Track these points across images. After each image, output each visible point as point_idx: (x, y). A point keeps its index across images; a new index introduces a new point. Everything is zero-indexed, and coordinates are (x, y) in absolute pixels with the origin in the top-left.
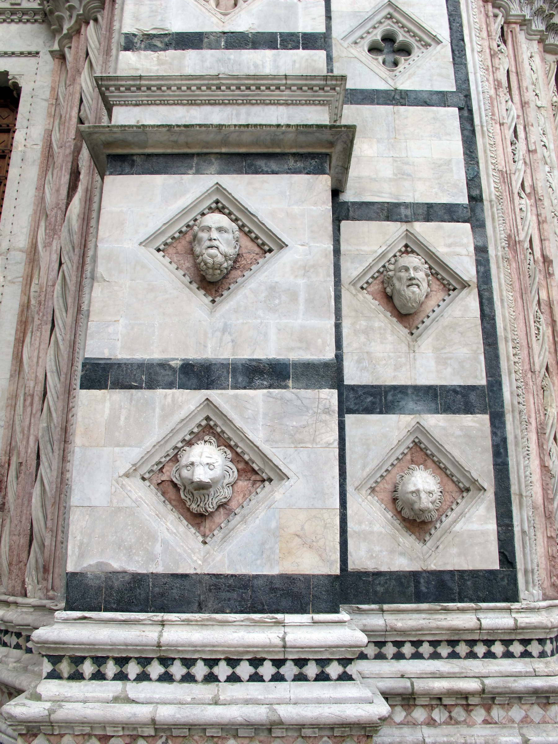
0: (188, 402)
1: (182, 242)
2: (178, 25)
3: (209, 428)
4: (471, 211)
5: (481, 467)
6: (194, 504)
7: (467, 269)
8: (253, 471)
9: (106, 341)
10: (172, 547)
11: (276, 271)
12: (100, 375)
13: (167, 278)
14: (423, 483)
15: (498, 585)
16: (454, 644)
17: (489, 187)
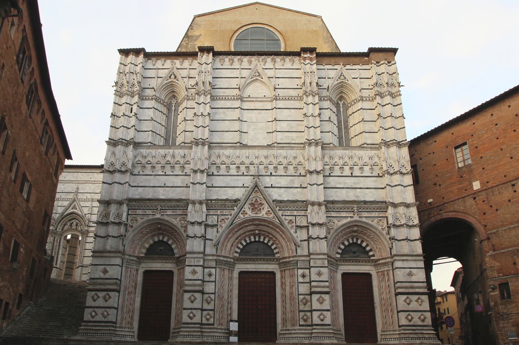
0: (190, 311)
1: (190, 298)
2: (190, 278)
3: (192, 313)
4: (214, 293)
5: (212, 315)
6: (191, 318)
7: (213, 299)
8: (194, 316)
9: (185, 306)
10: (189, 321)
11: (196, 301)
12: (185, 309)
13: (189, 301)
14: (208, 317)
15: (213, 325)
16: (209, 328)
17: (216, 291)
